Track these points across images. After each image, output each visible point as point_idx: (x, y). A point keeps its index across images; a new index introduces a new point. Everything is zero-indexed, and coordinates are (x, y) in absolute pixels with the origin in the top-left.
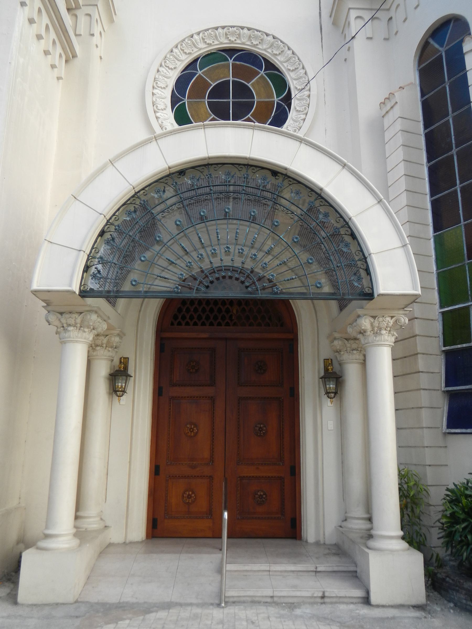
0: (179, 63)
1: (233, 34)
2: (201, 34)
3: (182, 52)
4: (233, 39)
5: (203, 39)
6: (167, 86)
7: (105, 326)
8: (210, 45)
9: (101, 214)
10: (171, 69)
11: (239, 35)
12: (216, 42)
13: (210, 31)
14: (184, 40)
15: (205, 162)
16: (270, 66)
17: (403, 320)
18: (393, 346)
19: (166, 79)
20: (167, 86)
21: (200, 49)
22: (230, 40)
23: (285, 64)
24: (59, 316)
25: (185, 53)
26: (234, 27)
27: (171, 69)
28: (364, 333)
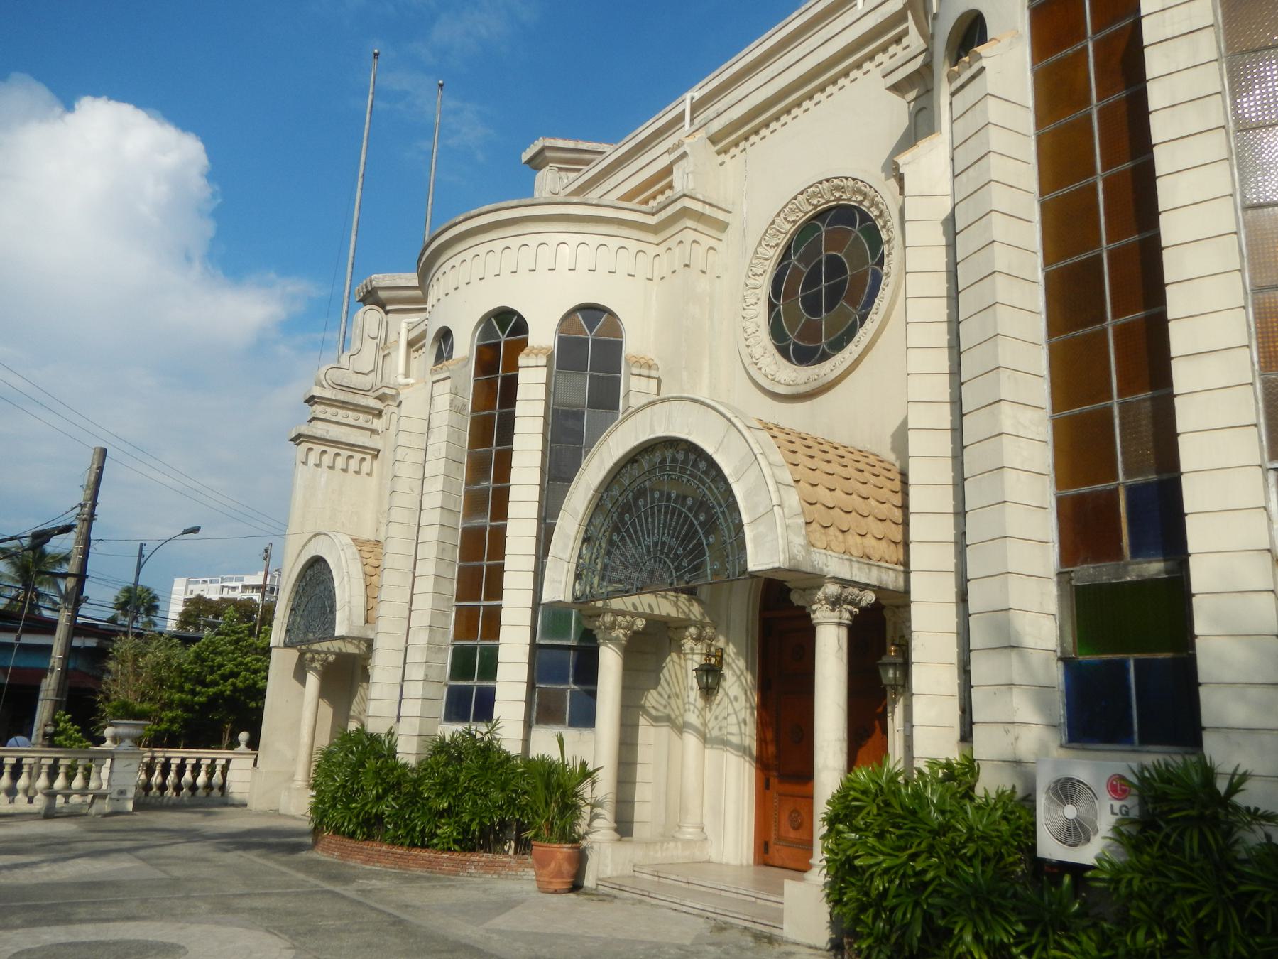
0: (766, 263)
1: (814, 195)
2: (782, 215)
3: (768, 248)
4: (815, 202)
5: (785, 219)
6: (758, 300)
8: (794, 222)
10: (761, 275)
11: (820, 193)
12: (801, 214)
13: (790, 206)
14: (766, 232)
16: (865, 217)
19: (757, 291)
20: (758, 300)
21: (786, 234)
22: (813, 205)
23: (872, 209)
25: (772, 247)
26: (811, 186)
27: (761, 275)
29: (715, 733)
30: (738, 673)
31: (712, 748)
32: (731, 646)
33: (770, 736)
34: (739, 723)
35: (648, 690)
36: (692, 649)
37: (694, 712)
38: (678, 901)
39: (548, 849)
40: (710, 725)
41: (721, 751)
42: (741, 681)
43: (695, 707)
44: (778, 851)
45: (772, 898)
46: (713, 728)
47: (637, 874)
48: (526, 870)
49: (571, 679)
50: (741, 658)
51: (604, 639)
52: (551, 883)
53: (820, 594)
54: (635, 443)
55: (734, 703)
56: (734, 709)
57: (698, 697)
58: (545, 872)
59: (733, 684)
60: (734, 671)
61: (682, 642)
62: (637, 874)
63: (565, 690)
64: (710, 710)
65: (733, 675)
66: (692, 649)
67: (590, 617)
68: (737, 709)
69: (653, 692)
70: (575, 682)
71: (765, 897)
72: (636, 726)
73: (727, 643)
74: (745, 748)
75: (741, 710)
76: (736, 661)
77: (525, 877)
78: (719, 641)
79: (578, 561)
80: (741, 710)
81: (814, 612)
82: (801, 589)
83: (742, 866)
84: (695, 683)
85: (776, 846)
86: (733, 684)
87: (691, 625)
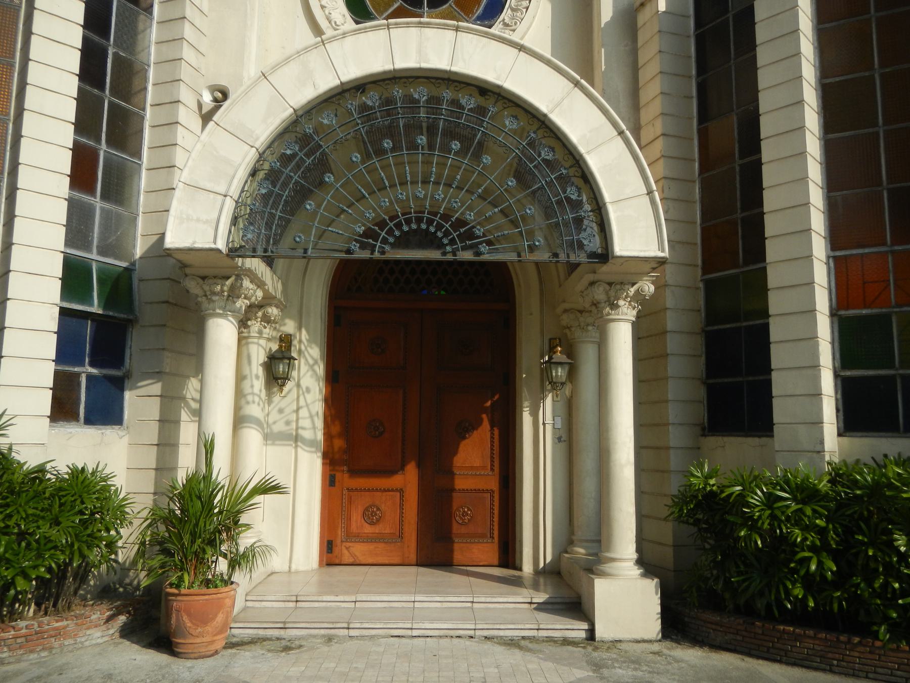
7: (260, 294)
9: (252, 147)
15: (391, 76)
17: (647, 288)
18: (633, 321)
24: (200, 281)
28: (598, 305)
29: (279, 427)
30: (311, 362)
31: (273, 444)
32: (304, 332)
33: (336, 429)
34: (311, 417)
35: (188, 377)
36: (260, 332)
37: (259, 404)
38: (409, 626)
39: (207, 597)
40: (271, 420)
41: (289, 448)
42: (314, 371)
43: (259, 397)
44: (347, 548)
45: (501, 600)
46: (274, 423)
47: (249, 604)
48: (88, 632)
49: (87, 360)
50: (313, 346)
51: (224, 309)
52: (213, 642)
53: (632, 290)
54: (389, 67)
55: (306, 394)
56: (306, 401)
57: (263, 388)
58: (209, 628)
59: (305, 375)
60: (306, 360)
61: (249, 323)
62: (249, 604)
63: (78, 375)
64: (270, 401)
65: (305, 364)
66: (260, 332)
67: (204, 278)
68: (309, 401)
69: (192, 379)
70: (92, 364)
71: (488, 600)
72: (177, 422)
73: (300, 329)
74: (317, 442)
75: (314, 402)
76: (309, 349)
77: (87, 643)
78: (285, 325)
79: (239, 198)
80: (314, 402)
81: (614, 307)
82: (605, 283)
83: (312, 570)
84: (260, 371)
85: (344, 544)
86: (305, 375)
87: (270, 305)
